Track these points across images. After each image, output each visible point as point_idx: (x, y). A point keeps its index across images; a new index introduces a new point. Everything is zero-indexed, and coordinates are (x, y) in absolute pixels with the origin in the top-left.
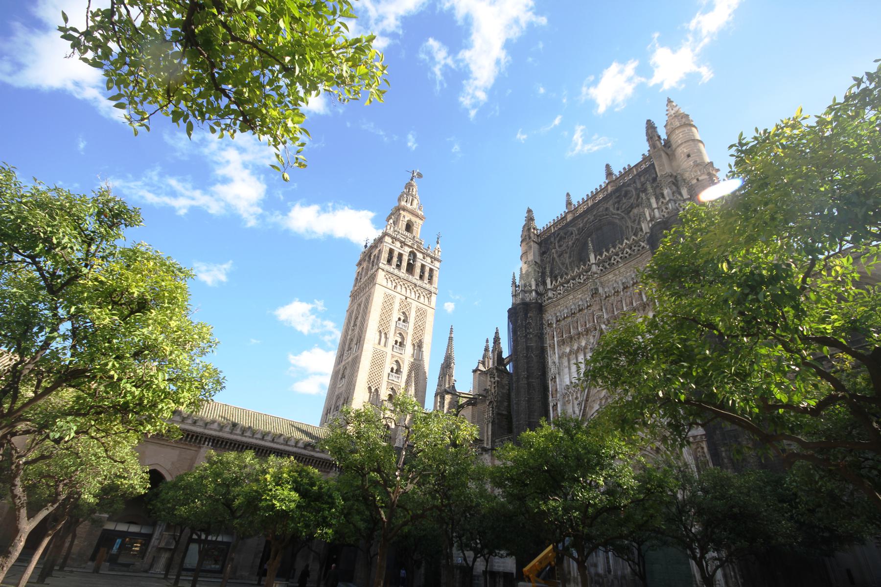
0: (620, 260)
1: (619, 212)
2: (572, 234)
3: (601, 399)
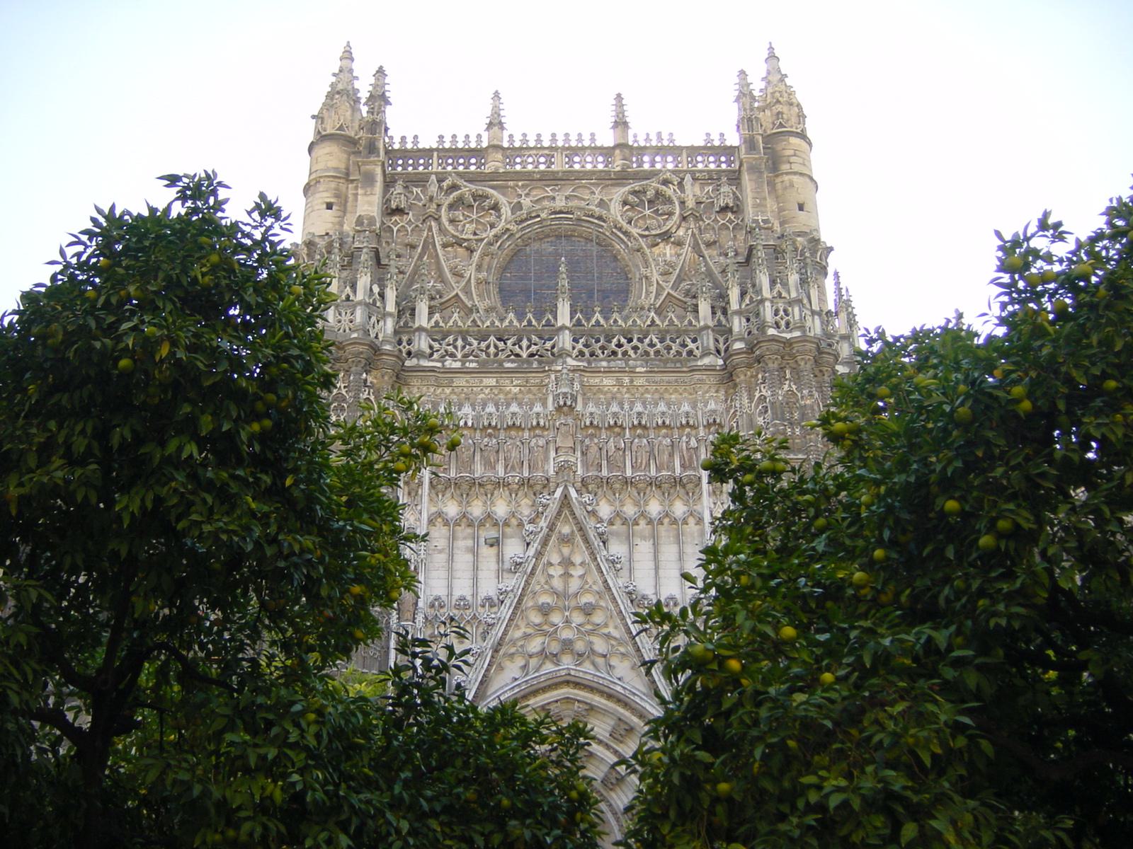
0: (631, 352)
1: (635, 231)
2: (496, 207)
3: (531, 656)
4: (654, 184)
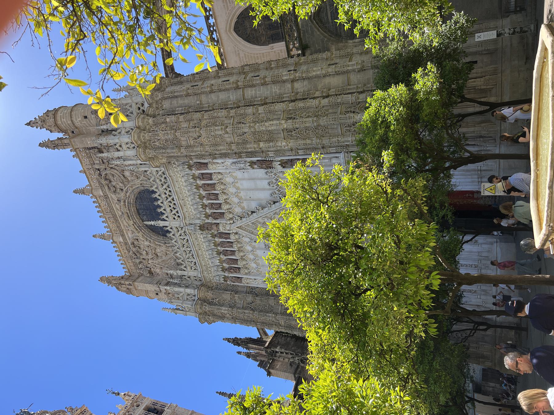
4: (104, 182)
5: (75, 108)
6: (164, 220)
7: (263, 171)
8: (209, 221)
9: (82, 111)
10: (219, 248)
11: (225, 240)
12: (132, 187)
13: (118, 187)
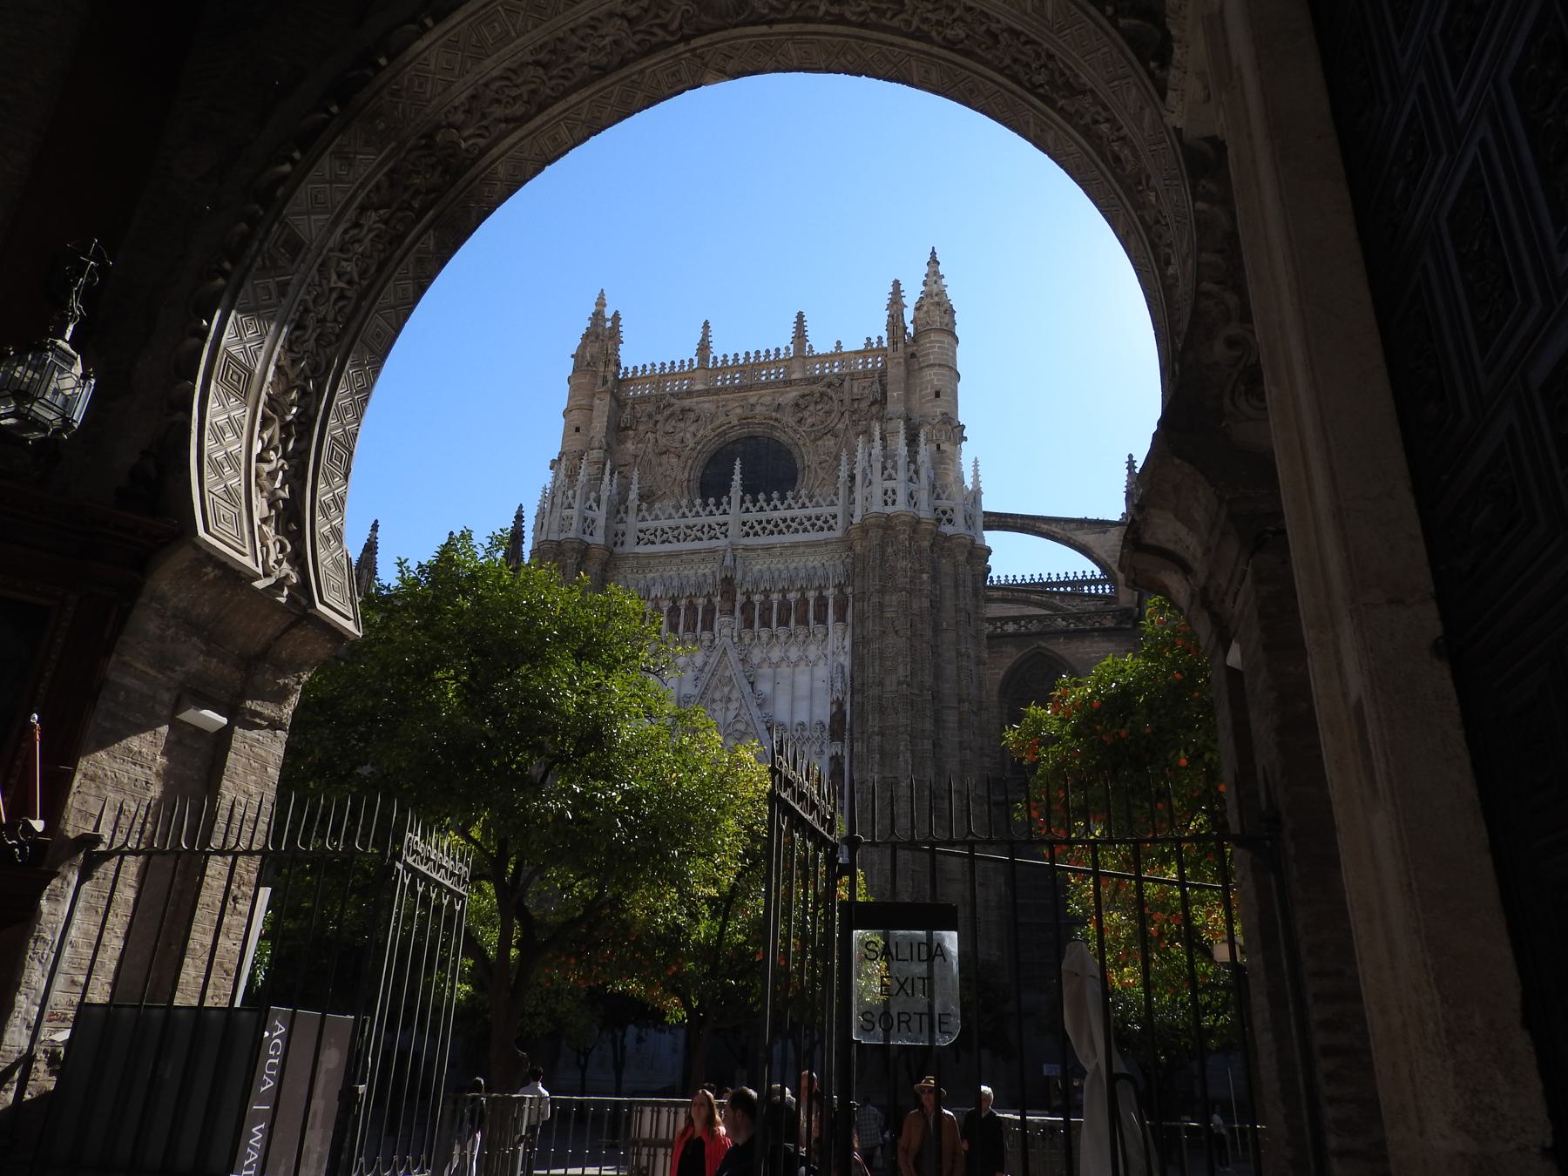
5: (953, 375)
6: (743, 501)
7: (827, 721)
8: (738, 596)
9: (949, 390)
10: (683, 602)
11: (700, 618)
12: (804, 445)
13: (806, 414)
